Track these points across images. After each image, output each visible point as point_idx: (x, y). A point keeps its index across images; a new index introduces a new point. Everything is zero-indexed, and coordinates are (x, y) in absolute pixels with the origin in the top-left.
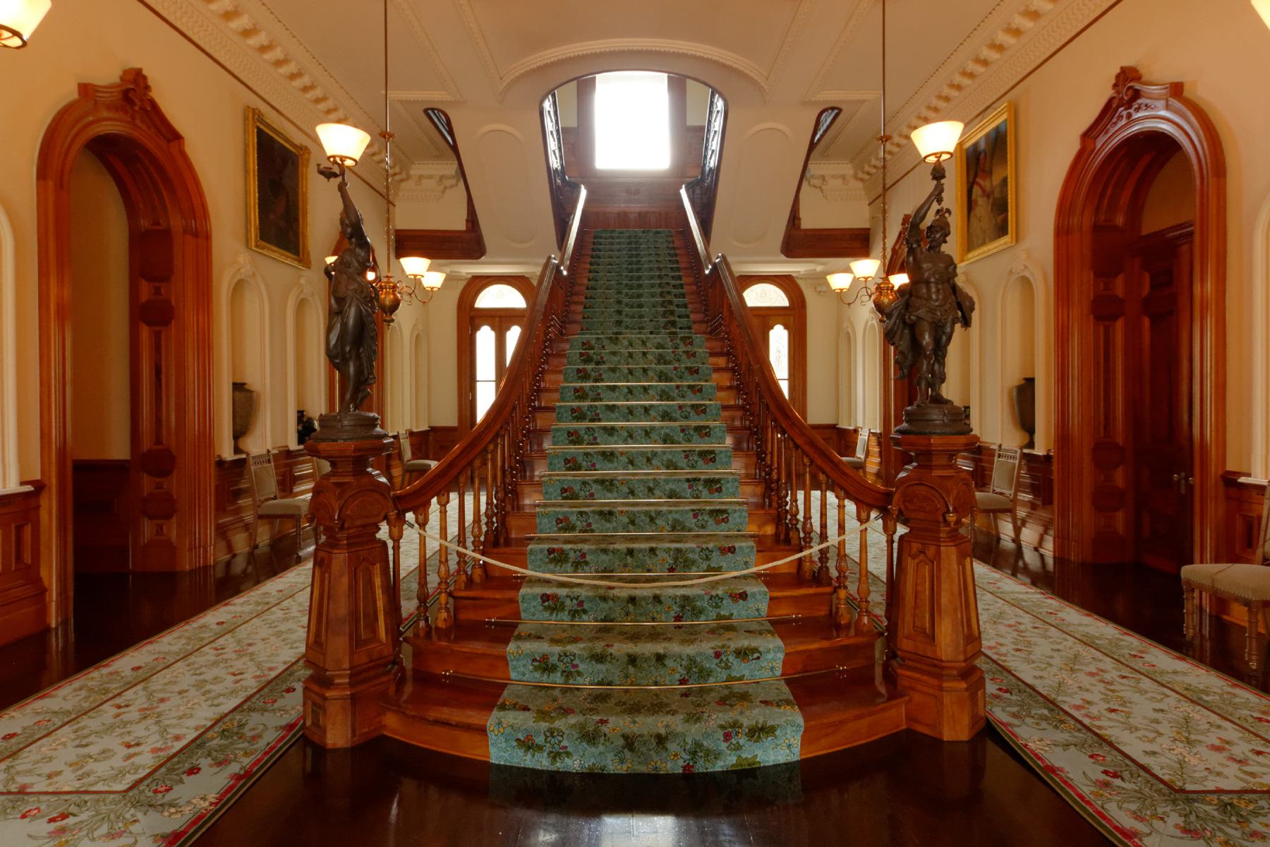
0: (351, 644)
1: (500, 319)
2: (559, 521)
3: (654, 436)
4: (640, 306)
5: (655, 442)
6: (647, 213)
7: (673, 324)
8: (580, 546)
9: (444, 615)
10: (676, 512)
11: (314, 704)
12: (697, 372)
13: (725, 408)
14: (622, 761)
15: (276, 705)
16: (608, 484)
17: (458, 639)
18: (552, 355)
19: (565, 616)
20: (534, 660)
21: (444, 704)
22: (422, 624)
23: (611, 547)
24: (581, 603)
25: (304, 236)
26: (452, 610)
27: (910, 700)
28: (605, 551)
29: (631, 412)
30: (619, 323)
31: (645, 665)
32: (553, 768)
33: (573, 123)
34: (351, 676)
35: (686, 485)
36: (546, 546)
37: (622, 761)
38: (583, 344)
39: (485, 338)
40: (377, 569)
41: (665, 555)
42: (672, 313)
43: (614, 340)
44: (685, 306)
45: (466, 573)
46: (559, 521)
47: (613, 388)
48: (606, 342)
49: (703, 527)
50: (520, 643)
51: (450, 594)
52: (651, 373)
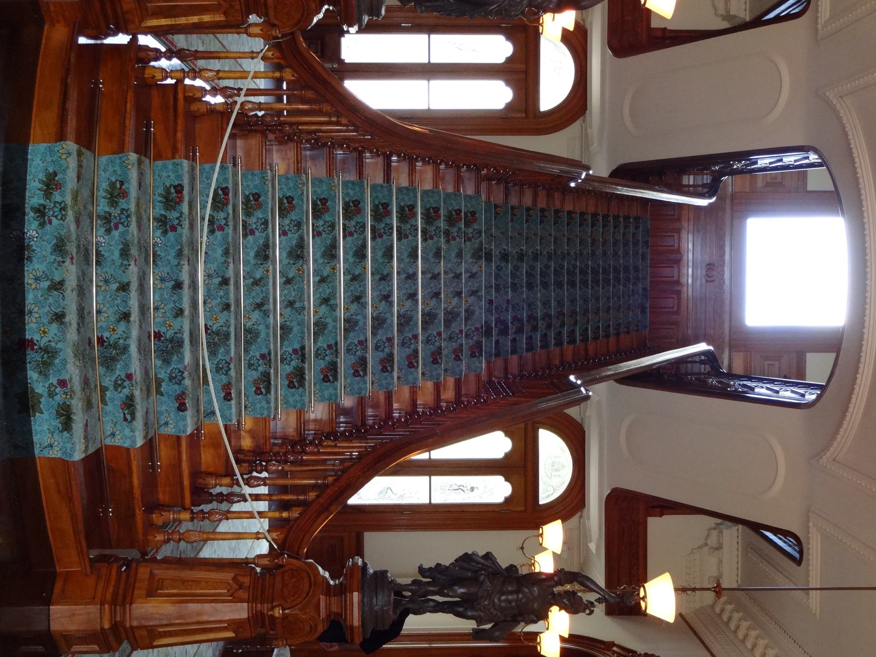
2: (256, 197)
3: (354, 307)
4: (530, 286)
5: (347, 309)
6: (679, 293)
7: (504, 332)
10: (268, 334)
12: (435, 362)
13: (389, 396)
16: (297, 253)
19: (160, 210)
20: (122, 183)
24: (174, 229)
27: (86, 575)
30: (505, 257)
31: (119, 301)
35: (297, 346)
36: (230, 186)
38: (473, 213)
41: (222, 321)
44: (530, 348)
46: (256, 197)
47: (413, 255)
48: (476, 243)
49: (250, 366)
52: (433, 302)
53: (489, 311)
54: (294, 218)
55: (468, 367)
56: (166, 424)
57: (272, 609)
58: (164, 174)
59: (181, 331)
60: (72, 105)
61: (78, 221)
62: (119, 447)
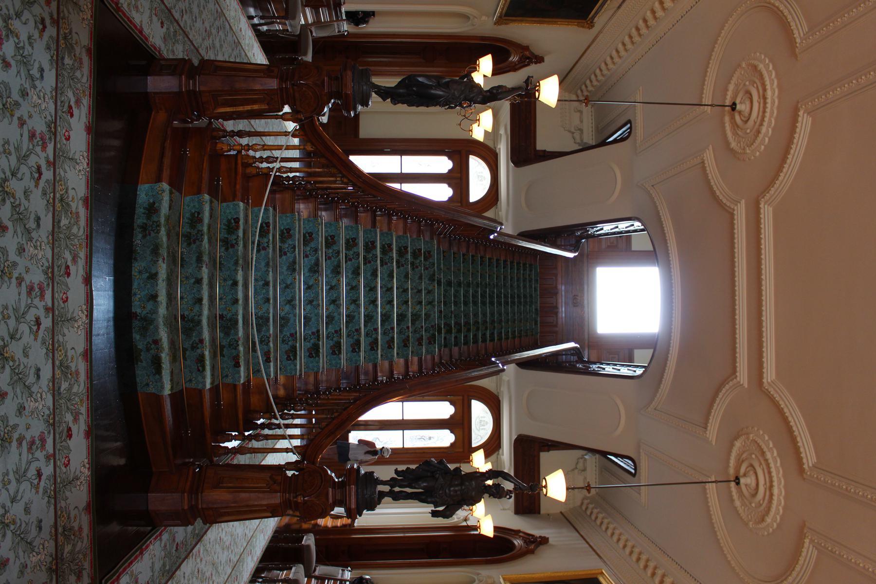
1: (458, 178)
2: (288, 230)
3: (352, 307)
5: (347, 309)
10: (295, 321)
13: (375, 366)
14: (140, 272)
16: (315, 269)
18: (420, 226)
24: (233, 246)
25: (522, 21)
28: (267, 265)
32: (135, 227)
33: (635, 246)
35: (314, 330)
36: (271, 222)
37: (140, 272)
38: (429, 252)
39: (442, 164)
41: (264, 310)
42: (459, 331)
46: (288, 230)
47: (391, 276)
49: (283, 341)
53: (440, 317)
55: (427, 351)
56: (227, 376)
57: (296, 497)
58: (228, 211)
59: (236, 314)
60: (167, 161)
61: (168, 235)
62: (195, 389)
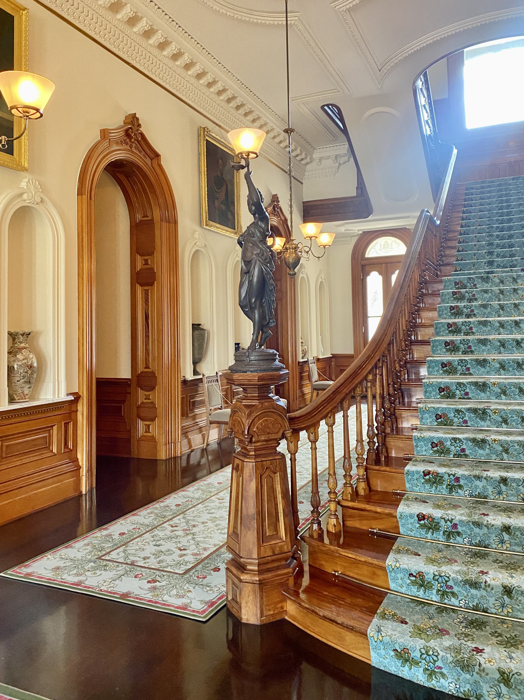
0: (258, 538)
8: (454, 470)
9: (333, 521)
11: (234, 583)
15: (205, 581)
17: (345, 546)
18: (427, 295)
21: (334, 601)
22: (315, 526)
23: (485, 474)
26: (340, 517)
29: (503, 345)
34: (259, 565)
38: (456, 283)
40: (277, 478)
43: (486, 280)
45: (351, 486)
47: (484, 323)
50: (398, 556)
51: (338, 503)
54: (453, 415)
